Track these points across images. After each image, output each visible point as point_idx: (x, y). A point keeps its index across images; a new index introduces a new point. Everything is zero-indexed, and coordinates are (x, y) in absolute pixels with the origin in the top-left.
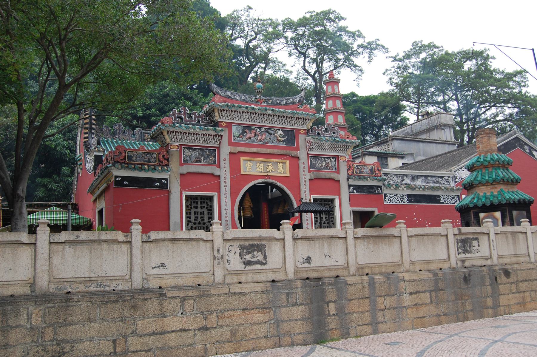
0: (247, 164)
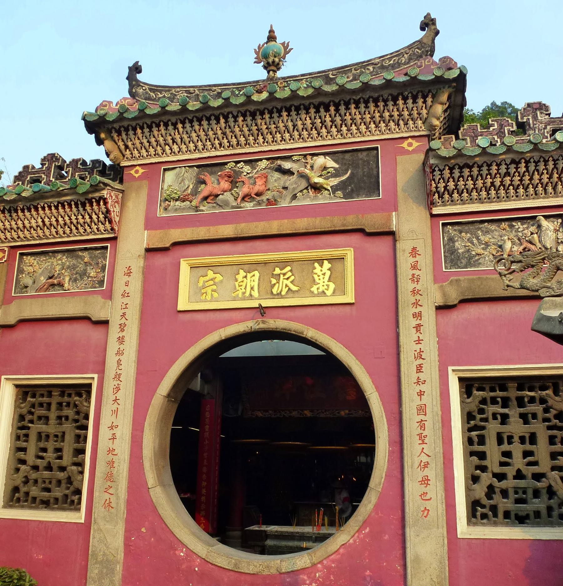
0: (202, 280)
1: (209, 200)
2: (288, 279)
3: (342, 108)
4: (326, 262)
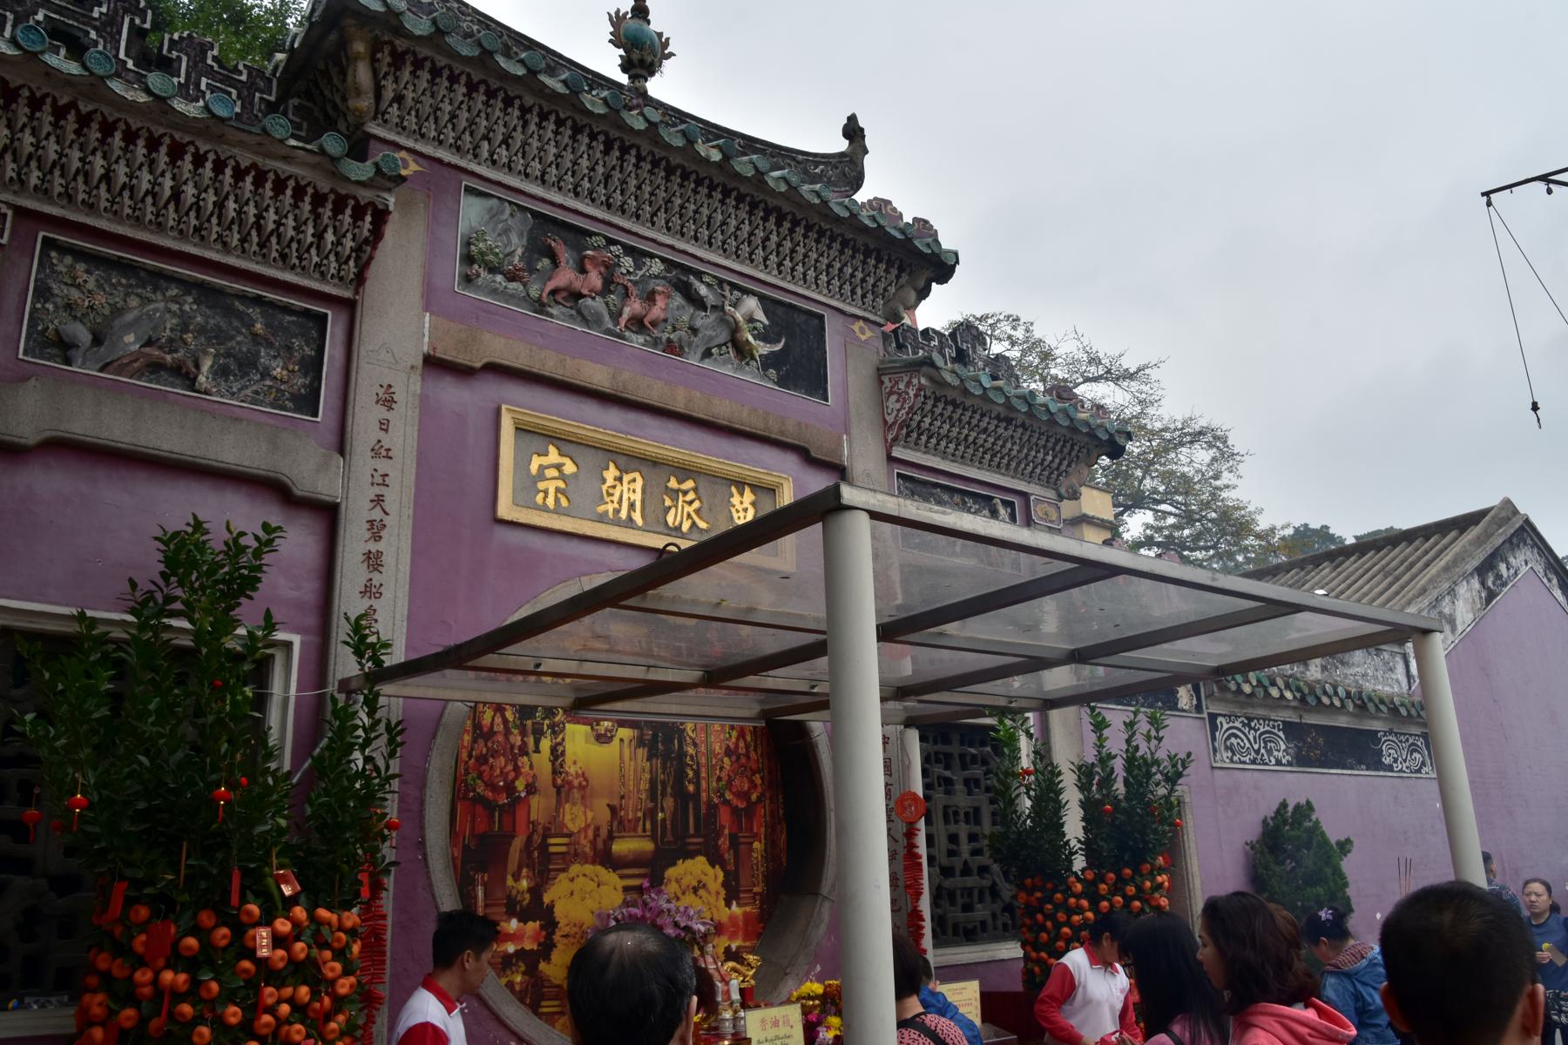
0: (536, 463)
1: (559, 298)
2: (691, 503)
3: (800, 230)
4: (747, 490)
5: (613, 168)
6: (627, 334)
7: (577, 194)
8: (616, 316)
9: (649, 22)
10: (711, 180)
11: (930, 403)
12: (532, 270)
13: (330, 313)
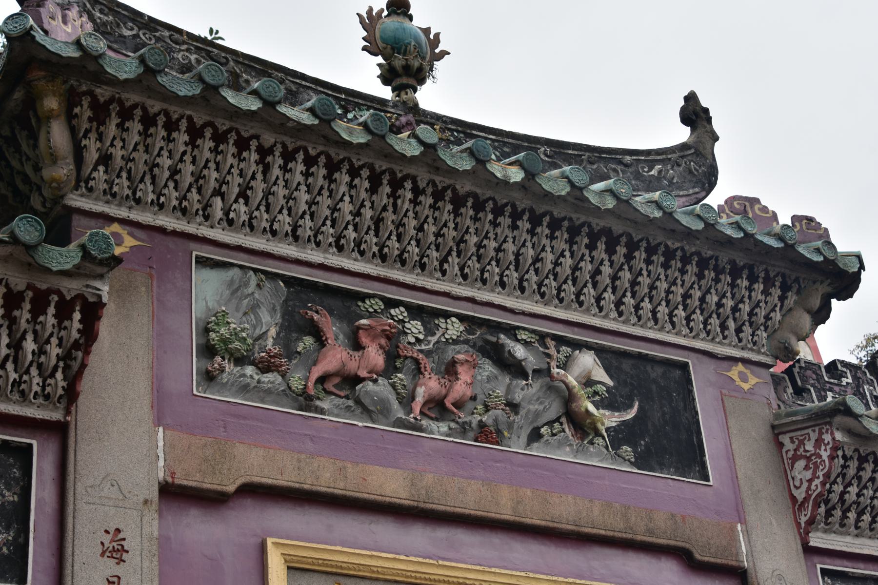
1: (329, 386)
3: (640, 255)
5: (385, 209)
6: (425, 422)
7: (340, 249)
8: (407, 401)
9: (411, 18)
10: (514, 206)
11: (853, 465)
12: (290, 354)
13: (34, 443)
